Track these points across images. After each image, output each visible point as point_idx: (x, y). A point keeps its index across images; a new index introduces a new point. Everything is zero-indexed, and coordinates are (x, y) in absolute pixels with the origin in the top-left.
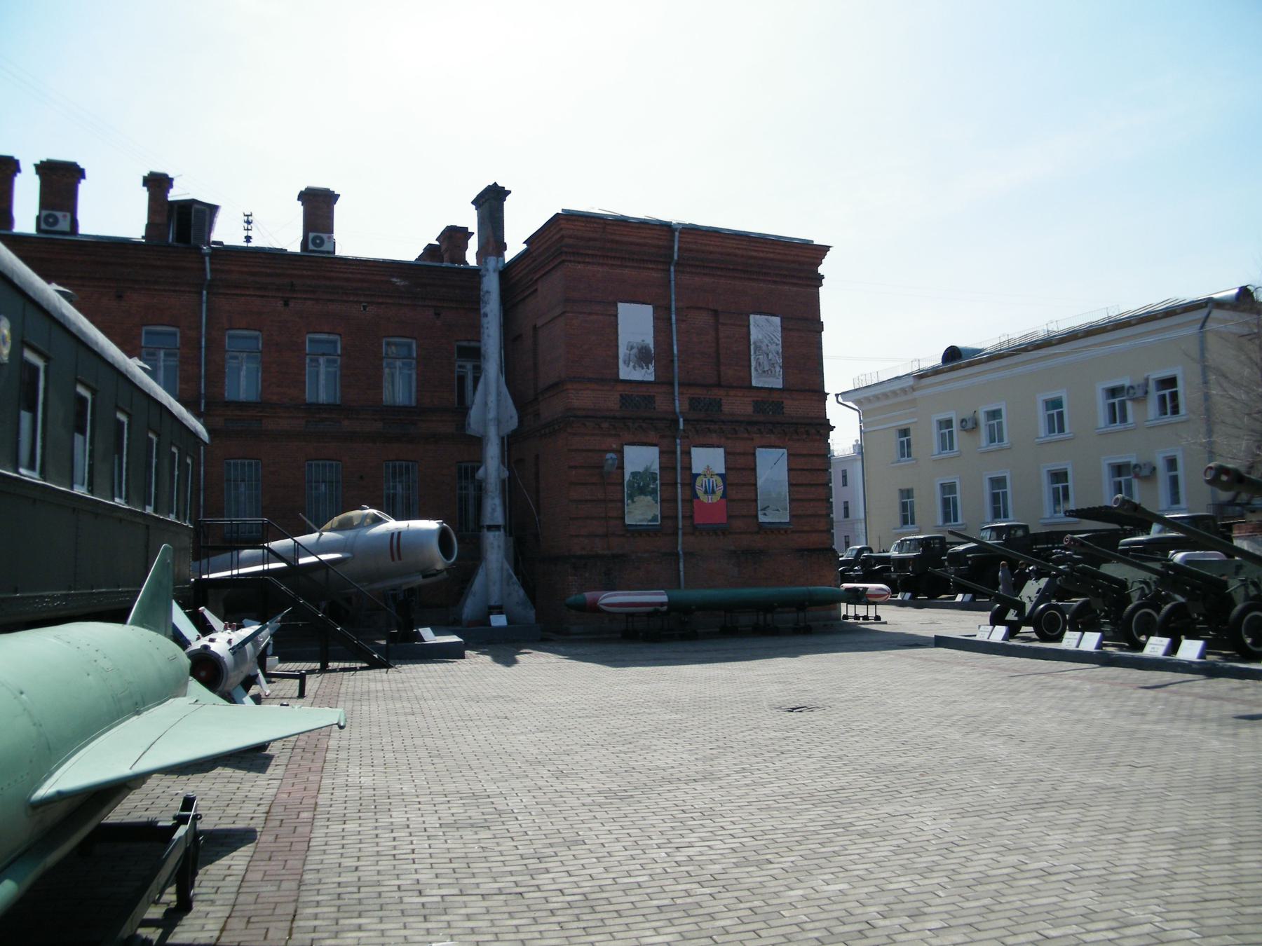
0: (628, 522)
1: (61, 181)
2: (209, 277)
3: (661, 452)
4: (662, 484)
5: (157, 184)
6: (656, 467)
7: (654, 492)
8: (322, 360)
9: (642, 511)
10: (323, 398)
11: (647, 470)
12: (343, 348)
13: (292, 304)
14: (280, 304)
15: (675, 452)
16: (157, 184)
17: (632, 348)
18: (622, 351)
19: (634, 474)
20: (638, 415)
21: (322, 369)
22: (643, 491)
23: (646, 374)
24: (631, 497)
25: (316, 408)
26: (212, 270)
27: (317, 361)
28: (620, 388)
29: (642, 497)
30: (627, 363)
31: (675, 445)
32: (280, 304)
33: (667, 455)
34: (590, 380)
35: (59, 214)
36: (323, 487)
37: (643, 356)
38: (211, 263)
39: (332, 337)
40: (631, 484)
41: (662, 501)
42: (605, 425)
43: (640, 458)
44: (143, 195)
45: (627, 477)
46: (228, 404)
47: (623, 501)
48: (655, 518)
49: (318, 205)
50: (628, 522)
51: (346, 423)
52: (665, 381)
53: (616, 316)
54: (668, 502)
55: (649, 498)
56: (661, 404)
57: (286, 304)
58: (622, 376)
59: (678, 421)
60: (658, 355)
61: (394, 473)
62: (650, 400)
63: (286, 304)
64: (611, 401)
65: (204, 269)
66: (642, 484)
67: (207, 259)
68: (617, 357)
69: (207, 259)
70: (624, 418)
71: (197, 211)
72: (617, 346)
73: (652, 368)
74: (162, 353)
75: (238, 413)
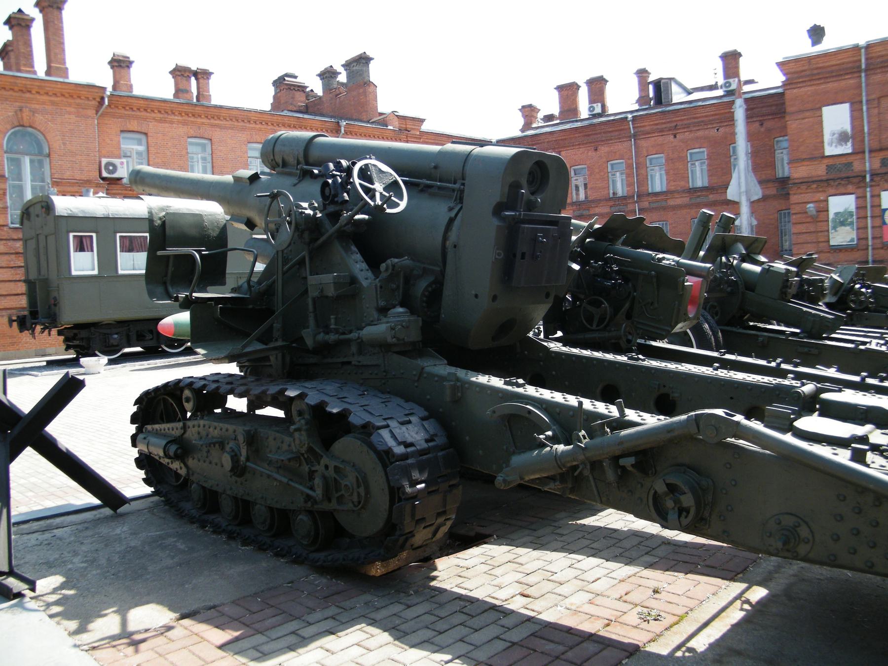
0: (832, 243)
1: (597, 86)
3: (857, 198)
4: (858, 218)
5: (642, 74)
6: (853, 208)
7: (851, 223)
8: (697, 163)
9: (842, 236)
10: (699, 183)
11: (846, 210)
15: (866, 197)
16: (642, 74)
17: (834, 134)
18: (827, 137)
19: (837, 214)
20: (841, 176)
21: (698, 169)
22: (843, 224)
23: (847, 148)
24: (834, 228)
28: (826, 161)
29: (843, 228)
30: (831, 144)
31: (865, 192)
33: (861, 198)
34: (804, 160)
35: (595, 105)
37: (843, 138)
39: (702, 150)
40: (834, 220)
41: (858, 229)
42: (815, 186)
43: (841, 203)
44: (635, 81)
45: (831, 216)
47: (828, 231)
48: (852, 240)
49: (731, 60)
50: (832, 243)
51: (711, 196)
52: (858, 152)
53: (821, 116)
54: (862, 228)
55: (848, 228)
56: (857, 167)
57: (675, 137)
58: (827, 153)
59: (865, 177)
60: (856, 135)
62: (850, 164)
63: (675, 137)
64: (819, 170)
66: (842, 220)
68: (823, 142)
70: (828, 180)
71: (664, 83)
72: (823, 135)
73: (849, 144)
74: (618, 174)
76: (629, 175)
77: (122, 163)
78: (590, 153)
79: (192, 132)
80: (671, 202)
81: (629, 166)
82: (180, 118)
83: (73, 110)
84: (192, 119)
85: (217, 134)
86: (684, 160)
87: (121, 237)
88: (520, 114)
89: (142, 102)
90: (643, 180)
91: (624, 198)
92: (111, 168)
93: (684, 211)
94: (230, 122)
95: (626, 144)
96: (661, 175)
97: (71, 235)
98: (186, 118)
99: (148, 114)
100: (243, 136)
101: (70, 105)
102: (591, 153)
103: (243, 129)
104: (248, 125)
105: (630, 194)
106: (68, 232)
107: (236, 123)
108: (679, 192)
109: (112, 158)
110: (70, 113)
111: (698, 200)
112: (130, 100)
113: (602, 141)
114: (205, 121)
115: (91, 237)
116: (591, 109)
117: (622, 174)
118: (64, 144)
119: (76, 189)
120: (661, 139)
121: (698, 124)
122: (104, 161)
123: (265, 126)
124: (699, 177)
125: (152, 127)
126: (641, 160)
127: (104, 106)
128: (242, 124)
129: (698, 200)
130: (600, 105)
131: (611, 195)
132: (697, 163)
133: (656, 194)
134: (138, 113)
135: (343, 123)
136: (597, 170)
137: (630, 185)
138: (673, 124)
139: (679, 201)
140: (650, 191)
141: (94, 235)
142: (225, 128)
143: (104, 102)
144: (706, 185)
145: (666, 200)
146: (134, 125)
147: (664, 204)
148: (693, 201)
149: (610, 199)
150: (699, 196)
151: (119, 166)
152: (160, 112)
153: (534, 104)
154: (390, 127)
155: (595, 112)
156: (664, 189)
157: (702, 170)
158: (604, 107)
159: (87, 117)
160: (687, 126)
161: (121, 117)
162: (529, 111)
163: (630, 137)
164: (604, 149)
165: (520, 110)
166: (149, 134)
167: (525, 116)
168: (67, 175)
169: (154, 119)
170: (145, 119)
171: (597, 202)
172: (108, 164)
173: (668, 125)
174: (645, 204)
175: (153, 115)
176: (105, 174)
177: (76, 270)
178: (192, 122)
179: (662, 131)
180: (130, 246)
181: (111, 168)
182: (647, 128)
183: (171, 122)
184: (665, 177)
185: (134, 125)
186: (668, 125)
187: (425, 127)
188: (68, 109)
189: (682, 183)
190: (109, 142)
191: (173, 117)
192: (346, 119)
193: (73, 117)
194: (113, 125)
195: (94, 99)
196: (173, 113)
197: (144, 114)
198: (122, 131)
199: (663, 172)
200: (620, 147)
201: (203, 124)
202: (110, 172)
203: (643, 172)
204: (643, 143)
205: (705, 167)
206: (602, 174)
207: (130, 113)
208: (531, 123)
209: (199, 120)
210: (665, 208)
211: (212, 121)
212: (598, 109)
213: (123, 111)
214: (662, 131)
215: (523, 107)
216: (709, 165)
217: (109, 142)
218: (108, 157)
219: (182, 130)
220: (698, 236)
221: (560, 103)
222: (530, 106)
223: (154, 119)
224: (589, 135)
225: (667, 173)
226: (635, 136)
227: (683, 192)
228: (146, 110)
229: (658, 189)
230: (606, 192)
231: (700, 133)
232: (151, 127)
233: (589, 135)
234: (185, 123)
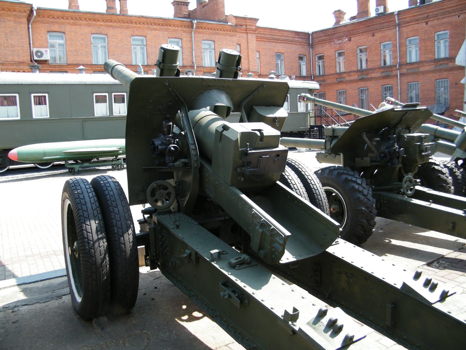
2: (397, 22)
12: (450, 35)
13: (429, 23)
14: (424, 24)
25: (440, 60)
26: (398, 19)
27: (440, 42)
32: (424, 25)
35: (379, 7)
36: (442, 89)
38: (398, 17)
39: (446, 32)
46: (407, 64)
51: (450, 64)
57: (427, 23)
61: (385, 90)
63: (427, 23)
65: (395, 20)
67: (396, 16)
69: (396, 16)
75: (410, 67)
76: (394, 52)
77: (46, 51)
78: (369, 38)
79: (94, 31)
80: (422, 69)
81: (395, 46)
82: (86, 22)
83: (11, 19)
84: (94, 22)
85: (111, 32)
86: (432, 40)
87: (34, 96)
88: (333, 16)
89: (60, 13)
90: (403, 55)
91: (390, 67)
92: (39, 54)
93: (431, 75)
94: (119, 24)
95: (393, 31)
96: (416, 51)
97: (33, 95)
98: (90, 22)
99: (65, 21)
100: (128, 32)
101: (9, 16)
102: (370, 38)
103: (128, 28)
104: (131, 25)
105: (395, 64)
106: (93, 93)
107: (123, 24)
108: (427, 62)
109: (40, 47)
110: (10, 21)
111: (441, 67)
112: (51, 12)
113: (377, 29)
114: (102, 23)
115: (45, 97)
116: (377, 10)
117: (390, 51)
118: (7, 40)
119: (15, 67)
120: (417, 26)
121: (444, 13)
122: (35, 50)
123: (143, 25)
124: (443, 51)
125: (68, 28)
126: (402, 41)
127: (34, 16)
128: (127, 24)
129: (441, 67)
130: (382, 7)
131: (382, 65)
132: (442, 42)
133: (411, 64)
134: (58, 20)
135: (195, 22)
136: (374, 49)
137: (395, 58)
138: (426, 15)
139: (427, 68)
140: (408, 61)
141: (47, 95)
142: (116, 27)
143: (33, 14)
144: (447, 56)
145: (418, 68)
146: (56, 28)
147: (417, 70)
148: (437, 68)
149: (382, 68)
150: (441, 64)
151: (44, 53)
152: (72, 19)
153: (342, 9)
154: (229, 24)
155: (379, 12)
156: (418, 60)
157: (445, 46)
158: (385, 8)
159: (21, 23)
160: (436, 16)
161: (47, 23)
162: (339, 14)
163: (396, 25)
164: (378, 35)
165: (333, 13)
166: (66, 33)
167: (336, 17)
168: (10, 58)
169: (69, 23)
170: (63, 24)
171: (373, 69)
172: (37, 52)
173: (422, 16)
174: (404, 71)
175: (68, 21)
176: (36, 58)
177: (17, 117)
178: (94, 25)
179: (418, 20)
180: (40, 101)
181: (39, 54)
182: (408, 19)
183: (81, 25)
184: (418, 52)
185: (56, 28)
186: (422, 16)
187: (259, 24)
188: (8, 18)
189: (430, 56)
190: (40, 38)
191: (81, 22)
192: (197, 19)
193: (12, 23)
194: (42, 28)
195: (25, 12)
196: (81, 19)
197: (62, 20)
198: (48, 32)
199: (418, 49)
200: (389, 33)
201: (101, 25)
202: (39, 57)
203: (403, 49)
204: (404, 30)
205: (447, 44)
206: (377, 51)
207: (53, 20)
208: (339, 22)
209: (98, 23)
210: (417, 73)
211: (107, 23)
212: (381, 10)
213: (48, 19)
214: (418, 20)
215: (335, 12)
216: (450, 42)
217: (40, 38)
218: (37, 47)
219: (87, 30)
220: (33, 83)
221: (358, 7)
222: (339, 11)
223: (69, 23)
224: (369, 26)
225: (420, 50)
226: (399, 25)
227: (431, 61)
228: (63, 18)
229: (414, 60)
230: (379, 63)
231: (446, 20)
232: (67, 28)
233: (369, 26)
234: (89, 25)
